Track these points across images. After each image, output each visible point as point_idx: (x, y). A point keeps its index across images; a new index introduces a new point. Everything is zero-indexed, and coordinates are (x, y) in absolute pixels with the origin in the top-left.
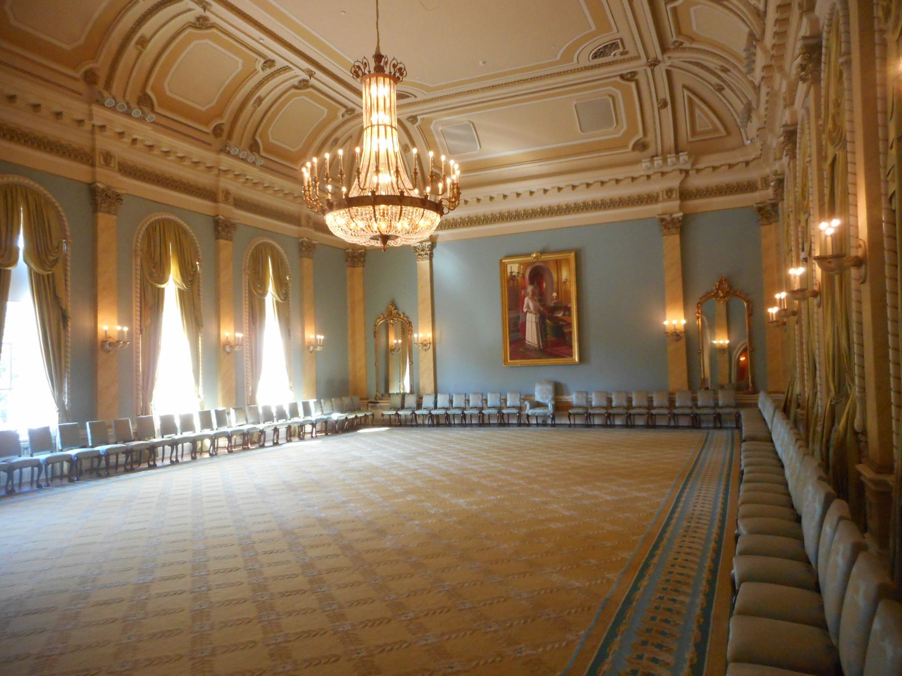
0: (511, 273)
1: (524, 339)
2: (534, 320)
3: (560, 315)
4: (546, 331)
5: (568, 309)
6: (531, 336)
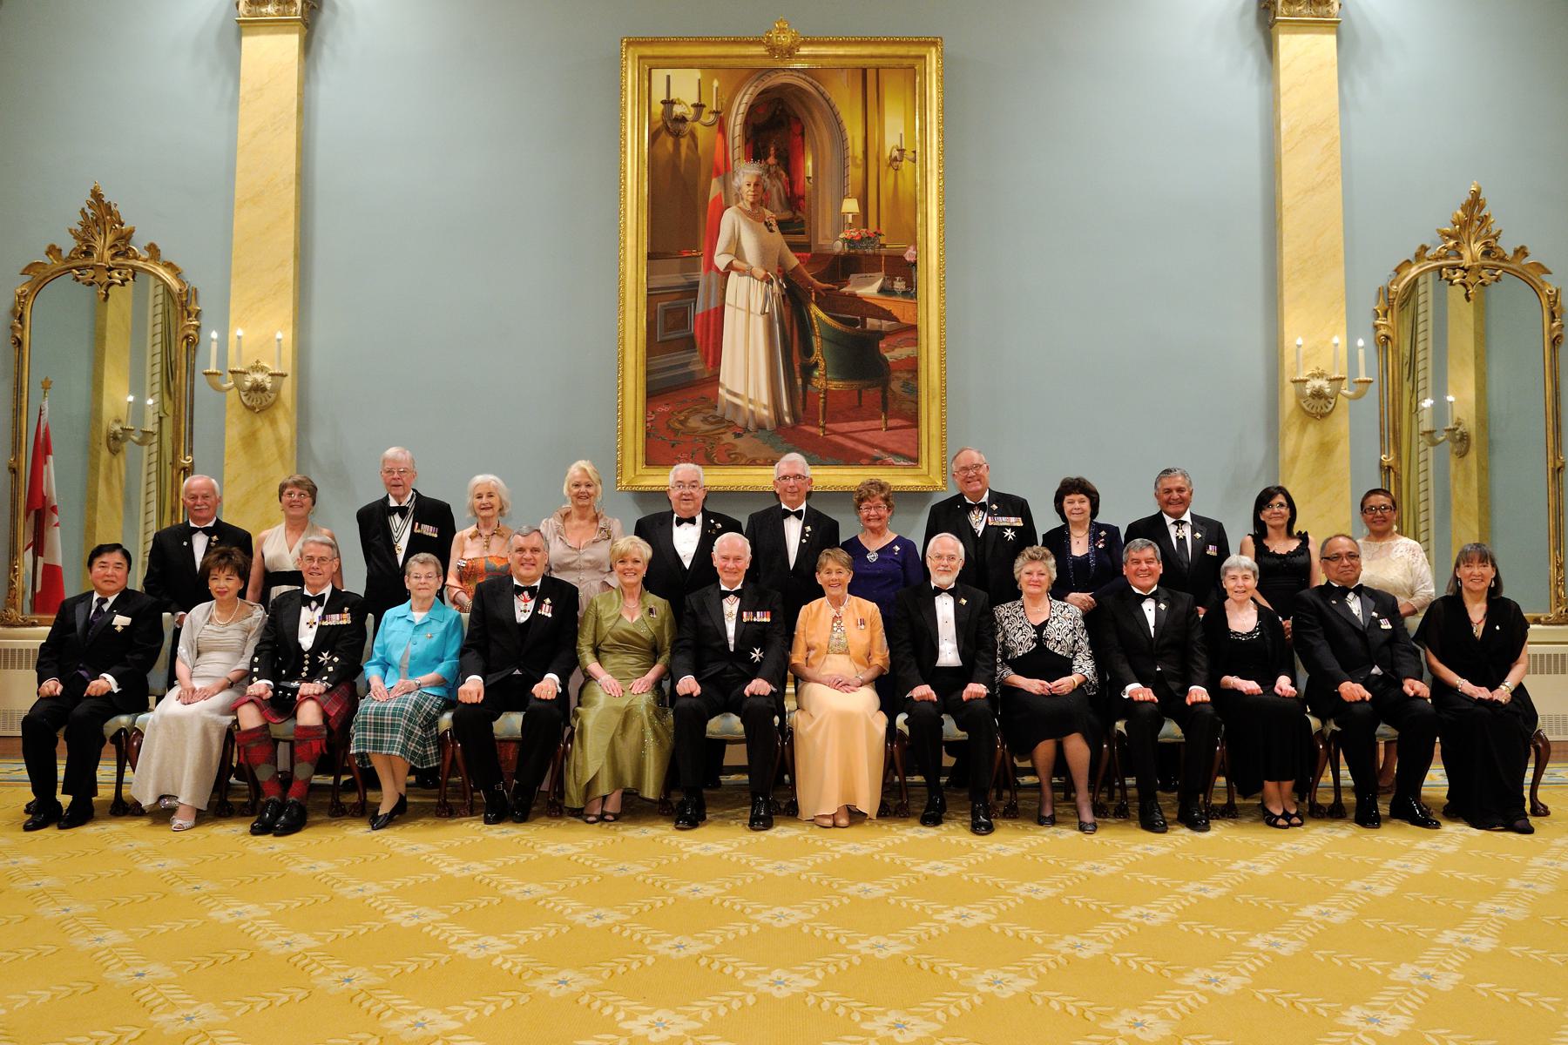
0: (669, 103)
1: (715, 379)
2: (757, 303)
3: (868, 289)
4: (807, 350)
5: (903, 270)
6: (746, 369)
